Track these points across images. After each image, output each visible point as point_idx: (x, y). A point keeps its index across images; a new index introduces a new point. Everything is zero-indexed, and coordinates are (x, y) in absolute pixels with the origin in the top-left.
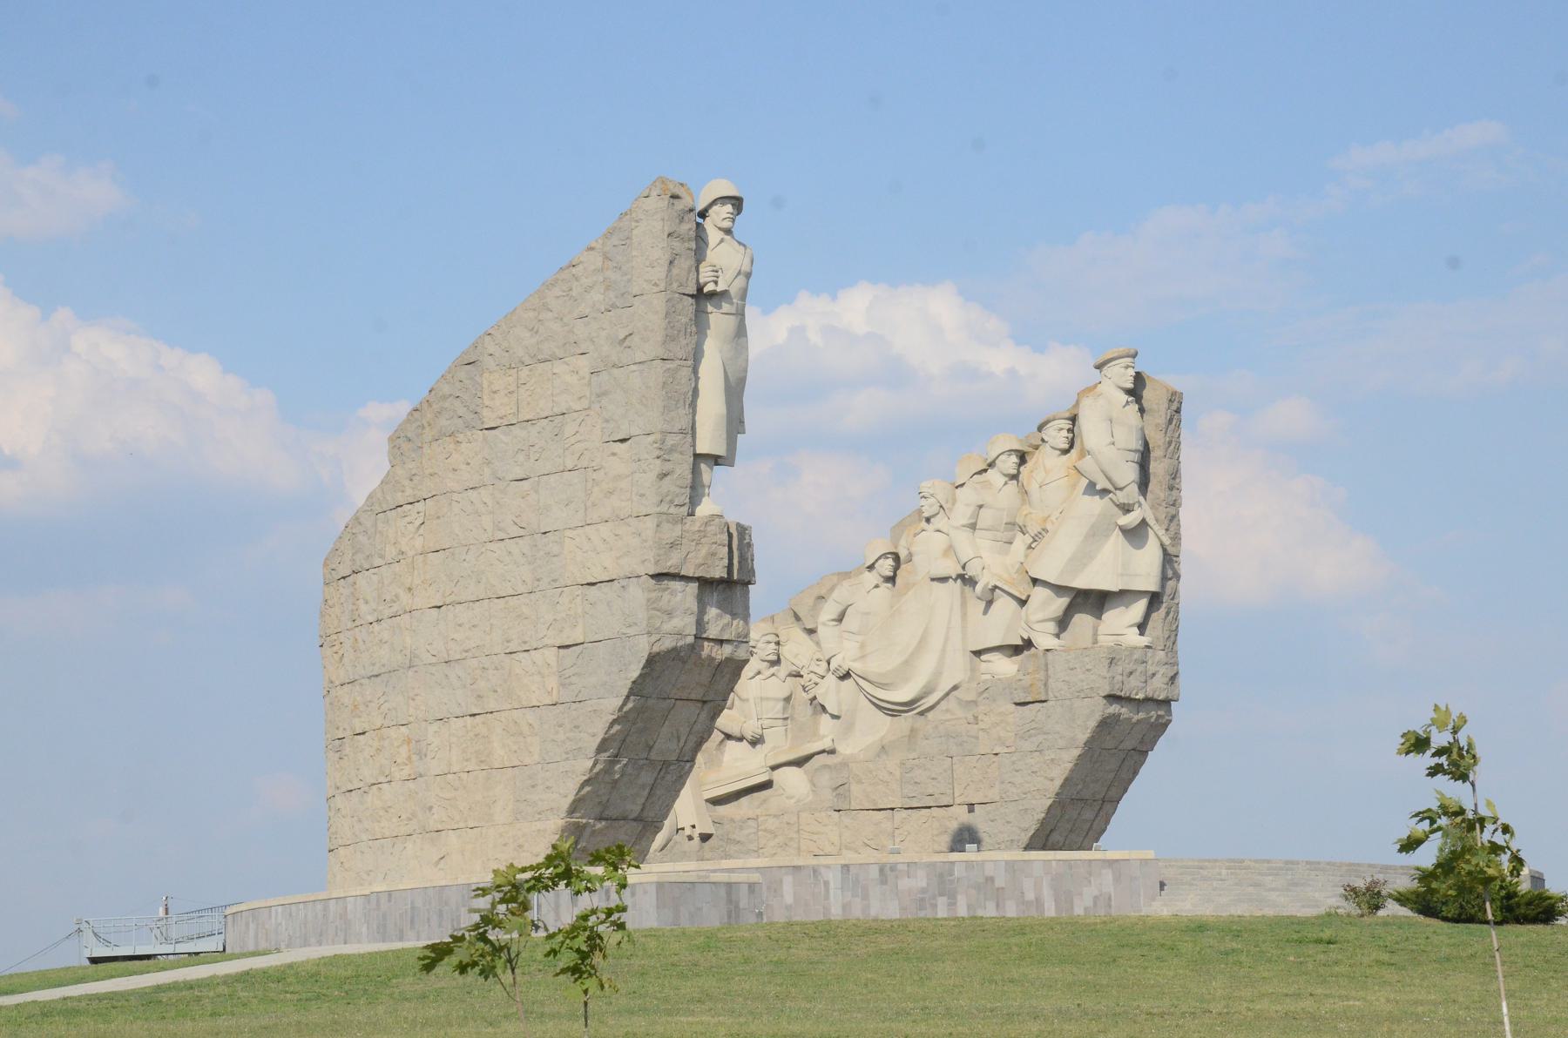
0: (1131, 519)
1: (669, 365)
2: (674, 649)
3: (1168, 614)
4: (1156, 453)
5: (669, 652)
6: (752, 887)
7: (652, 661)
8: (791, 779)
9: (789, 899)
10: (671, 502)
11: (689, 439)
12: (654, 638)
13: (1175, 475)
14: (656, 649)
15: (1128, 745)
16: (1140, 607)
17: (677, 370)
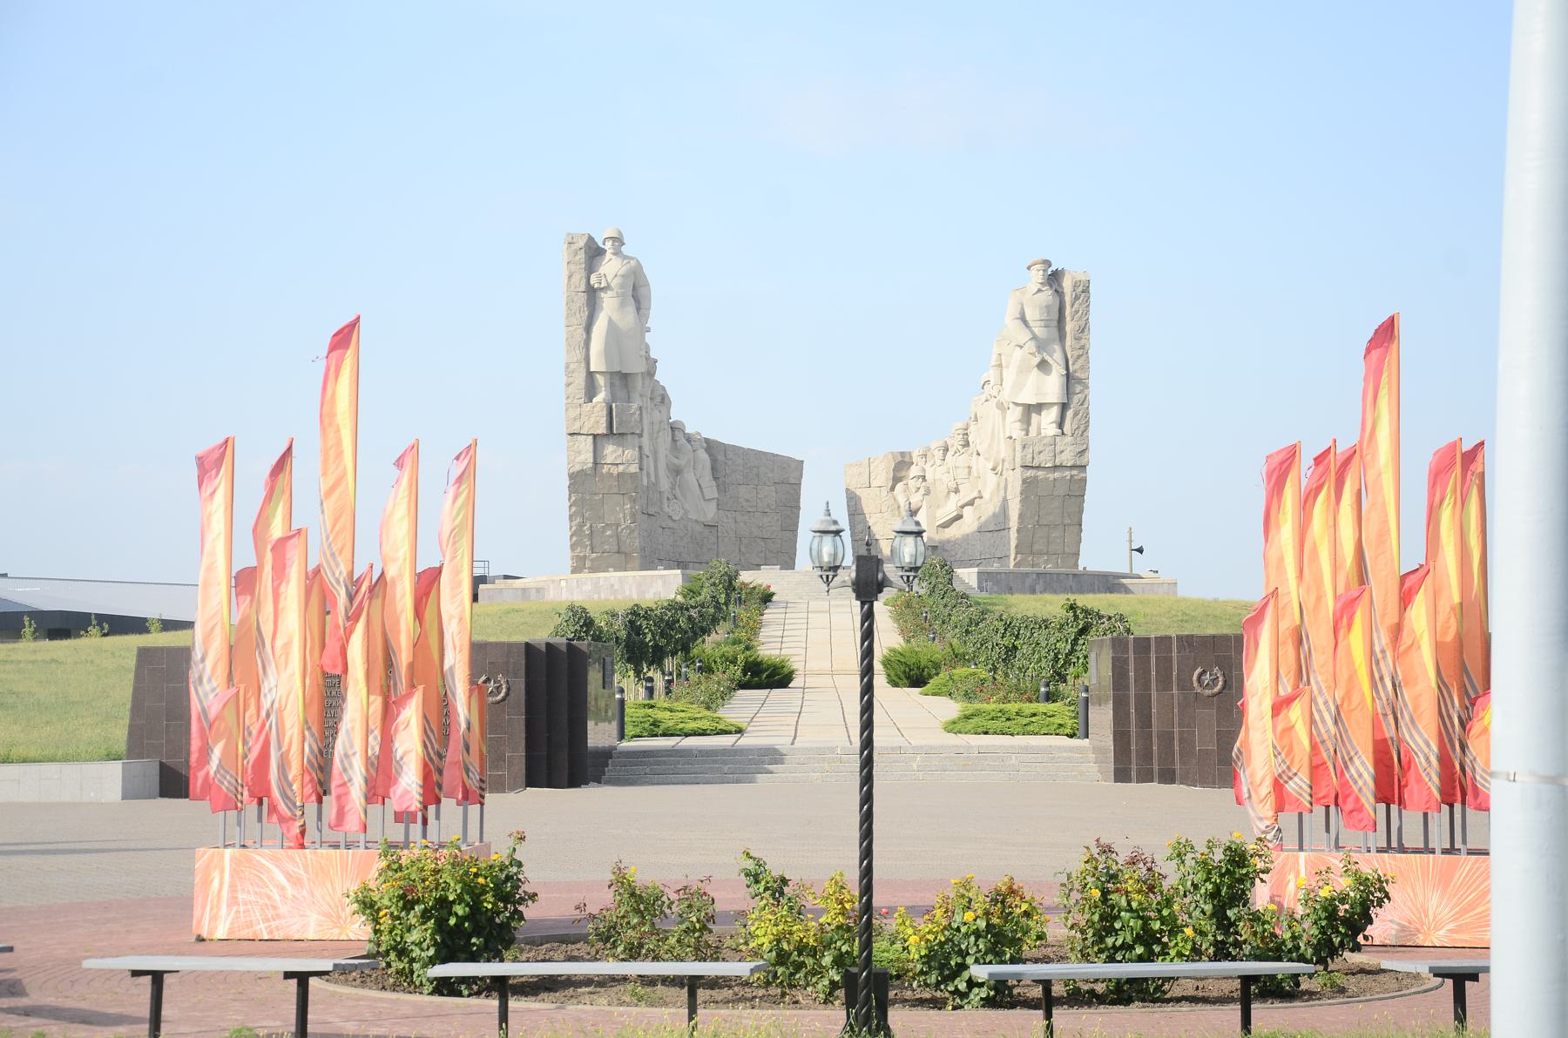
0: (1037, 360)
3: (1076, 414)
4: (1068, 319)
6: (538, 590)
7: (571, 476)
8: (967, 511)
13: (1083, 329)
15: (1061, 490)
16: (1054, 413)
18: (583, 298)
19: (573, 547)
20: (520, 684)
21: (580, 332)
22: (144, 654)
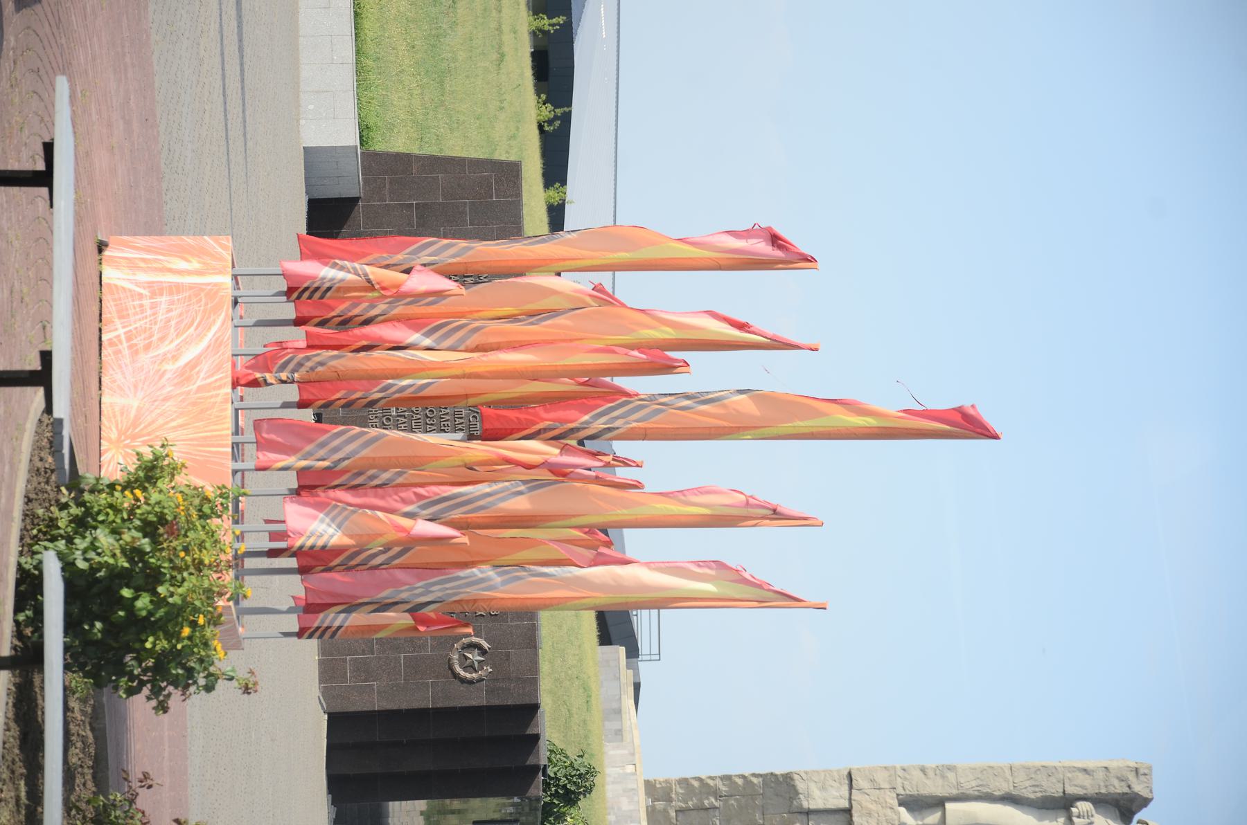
1: (1008, 772)
2: (797, 793)
5: (794, 786)
6: (619, 733)
7: (788, 777)
9: (611, 752)
10: (905, 779)
11: (955, 792)
12: (803, 775)
14: (796, 777)
17: (1006, 780)
18: (1055, 790)
19: (684, 782)
20: (478, 699)
21: (1002, 787)
22: (510, 172)
